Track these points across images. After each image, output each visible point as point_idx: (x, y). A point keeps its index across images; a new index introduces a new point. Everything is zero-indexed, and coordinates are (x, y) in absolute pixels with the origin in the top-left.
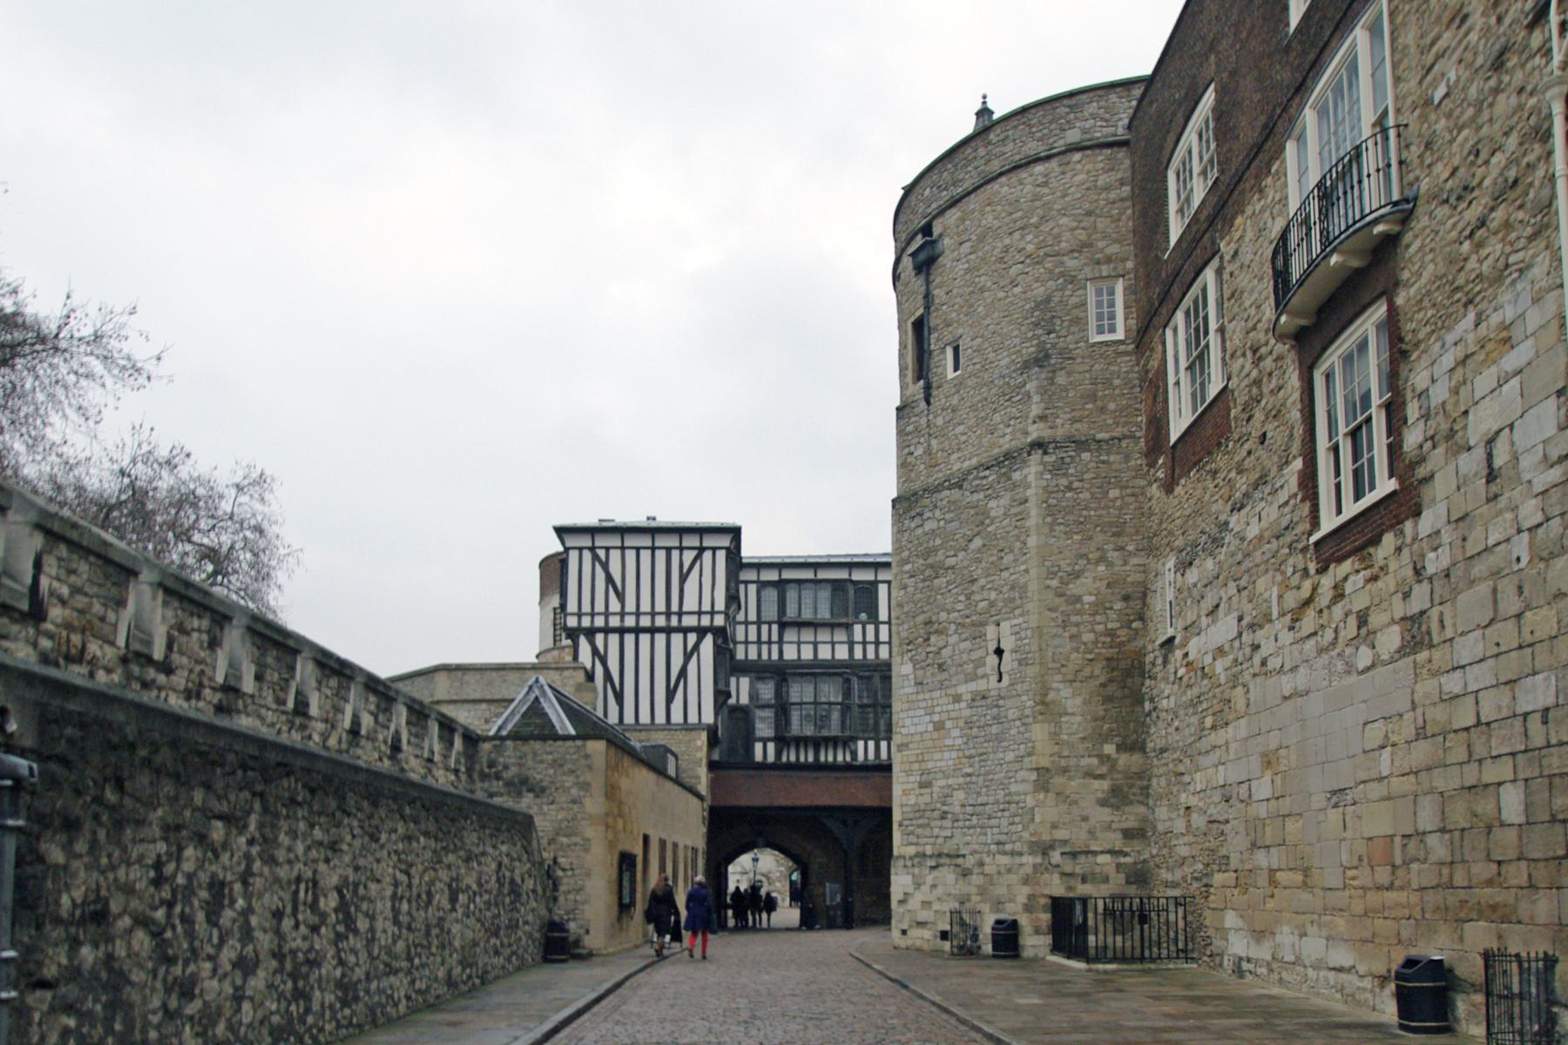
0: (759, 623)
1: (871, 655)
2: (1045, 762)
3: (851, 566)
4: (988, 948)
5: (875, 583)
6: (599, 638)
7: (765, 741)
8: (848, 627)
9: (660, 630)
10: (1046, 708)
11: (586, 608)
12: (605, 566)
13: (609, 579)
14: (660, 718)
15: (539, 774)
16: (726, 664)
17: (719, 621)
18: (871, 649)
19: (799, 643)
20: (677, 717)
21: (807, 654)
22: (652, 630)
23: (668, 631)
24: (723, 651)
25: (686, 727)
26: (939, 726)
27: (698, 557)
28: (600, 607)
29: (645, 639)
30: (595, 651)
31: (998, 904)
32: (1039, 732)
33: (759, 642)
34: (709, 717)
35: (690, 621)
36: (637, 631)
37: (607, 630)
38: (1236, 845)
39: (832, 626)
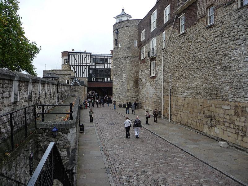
0: (93, 63)
1: (107, 68)
2: (128, 89)
3: (104, 56)
4: (123, 107)
5: (107, 58)
6: (74, 66)
7: (94, 78)
8: (104, 64)
9: (82, 65)
10: (129, 84)
11: (72, 62)
12: (74, 57)
13: (75, 59)
14: (82, 76)
15: (78, 90)
16: (90, 69)
17: (89, 64)
18: (107, 67)
19: (98, 66)
20: (84, 76)
21: (99, 67)
22: (81, 65)
23: (83, 65)
24: (89, 68)
25: (85, 77)
26: (118, 84)
27: (86, 56)
28: (74, 62)
29: (80, 66)
30: (73, 68)
31: (124, 103)
32: (128, 86)
33: (93, 66)
34: (88, 76)
35: (85, 64)
36: (79, 65)
37: (75, 65)
38: (145, 99)
39: (102, 64)
